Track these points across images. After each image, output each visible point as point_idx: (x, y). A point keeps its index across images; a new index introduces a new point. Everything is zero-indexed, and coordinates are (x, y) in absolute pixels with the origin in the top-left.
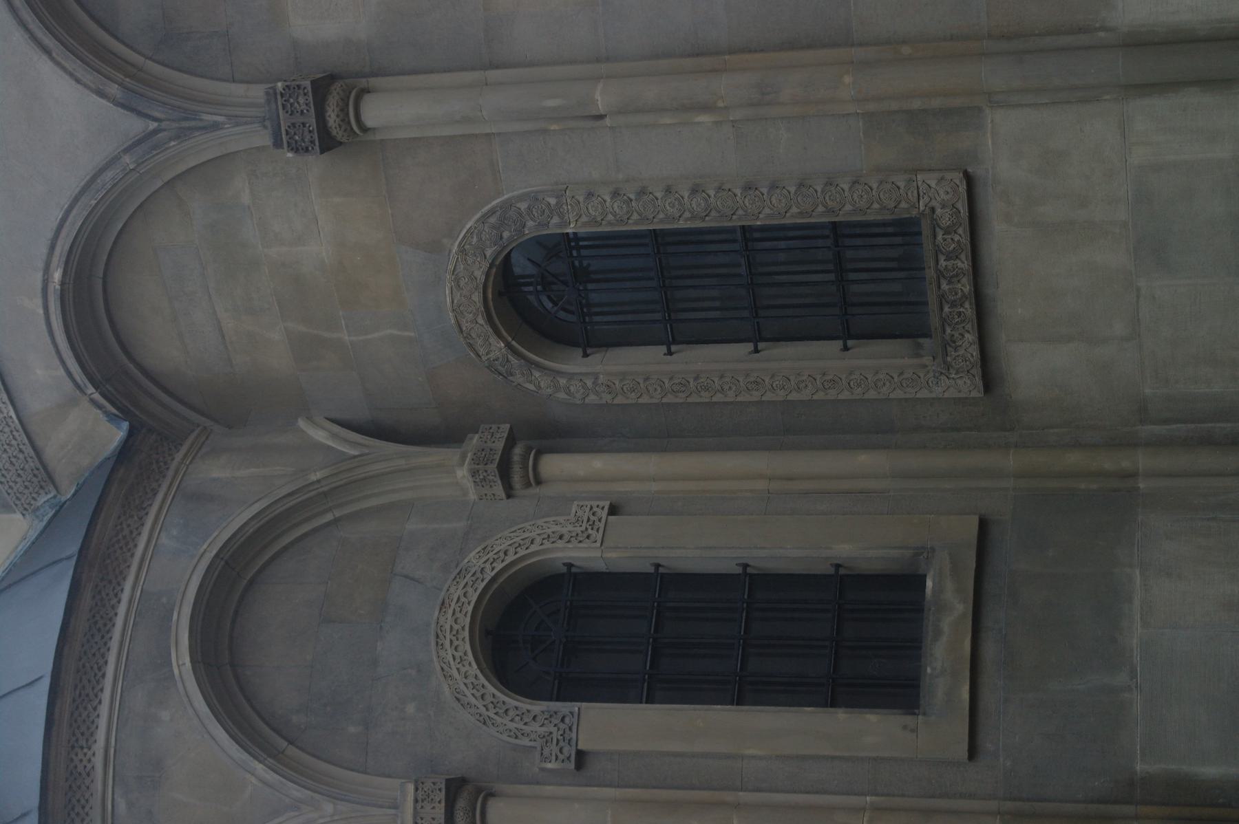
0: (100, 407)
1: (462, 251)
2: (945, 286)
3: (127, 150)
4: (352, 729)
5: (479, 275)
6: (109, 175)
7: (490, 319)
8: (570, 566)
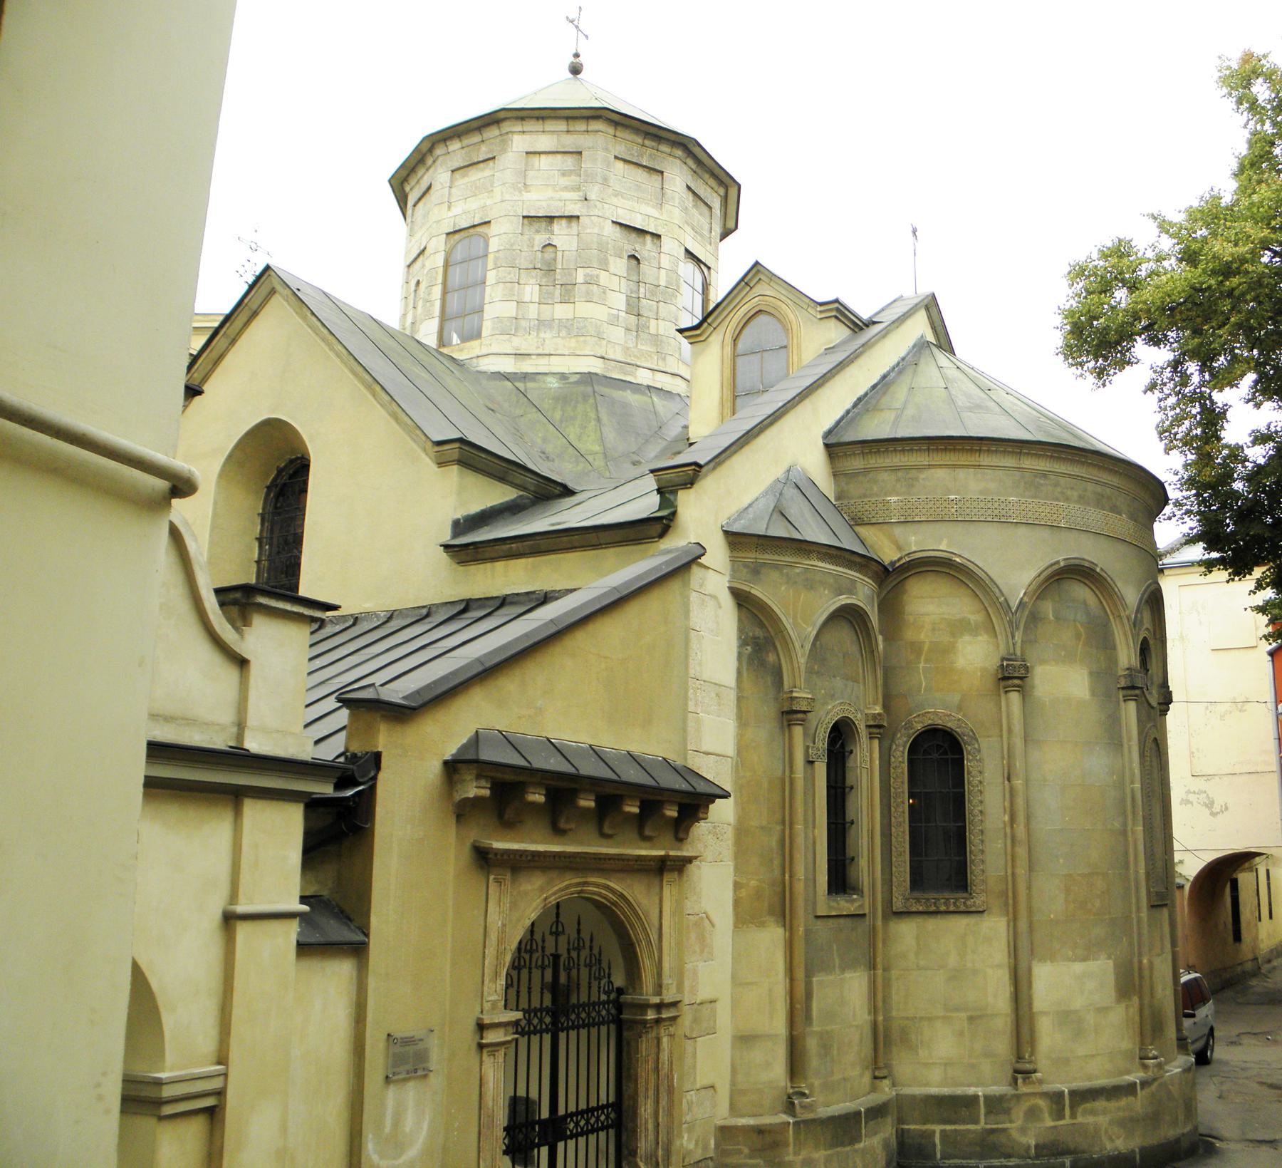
0: (900, 559)
1: (959, 720)
2: (942, 901)
3: (1005, 599)
4: (816, 667)
5: (949, 725)
6: (997, 591)
8: (851, 752)
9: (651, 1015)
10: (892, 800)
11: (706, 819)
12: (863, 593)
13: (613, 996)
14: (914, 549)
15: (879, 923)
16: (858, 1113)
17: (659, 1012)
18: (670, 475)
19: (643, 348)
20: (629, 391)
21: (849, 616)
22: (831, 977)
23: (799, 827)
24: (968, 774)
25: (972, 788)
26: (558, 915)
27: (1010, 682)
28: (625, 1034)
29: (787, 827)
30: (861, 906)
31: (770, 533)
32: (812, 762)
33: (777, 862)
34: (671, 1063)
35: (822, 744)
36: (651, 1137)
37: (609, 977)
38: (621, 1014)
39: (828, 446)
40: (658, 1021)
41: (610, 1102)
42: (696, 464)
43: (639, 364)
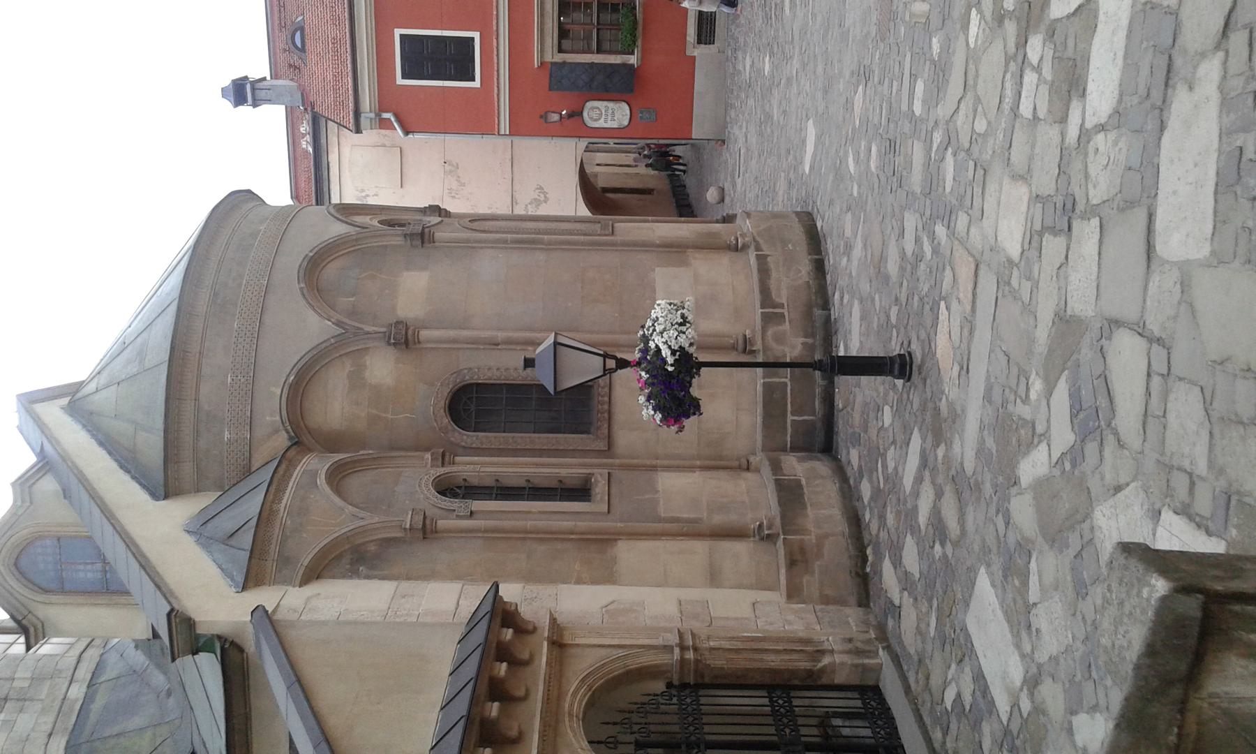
0: (288, 432)
1: (442, 385)
2: (600, 407)
4: (384, 508)
5: (446, 394)
7: (445, 411)
8: (465, 480)
9: (690, 655)
10: (510, 447)
11: (517, 605)
12: (316, 464)
13: (674, 692)
14: (278, 418)
15: (617, 461)
16: (776, 480)
17: (688, 648)
18: (180, 642)
19: (45, 691)
20: (92, 706)
21: (337, 477)
22: (662, 502)
23: (529, 524)
24: (490, 379)
25: (503, 377)
26: (599, 742)
27: (410, 337)
28: (707, 680)
29: (530, 536)
30: (601, 475)
31: (249, 547)
32: (471, 512)
33: (559, 546)
34: (732, 639)
35: (455, 504)
36: (795, 656)
37: (657, 695)
38: (689, 684)
39: (166, 497)
40: (696, 649)
41: (766, 695)
42: (169, 615)
43: (62, 697)
